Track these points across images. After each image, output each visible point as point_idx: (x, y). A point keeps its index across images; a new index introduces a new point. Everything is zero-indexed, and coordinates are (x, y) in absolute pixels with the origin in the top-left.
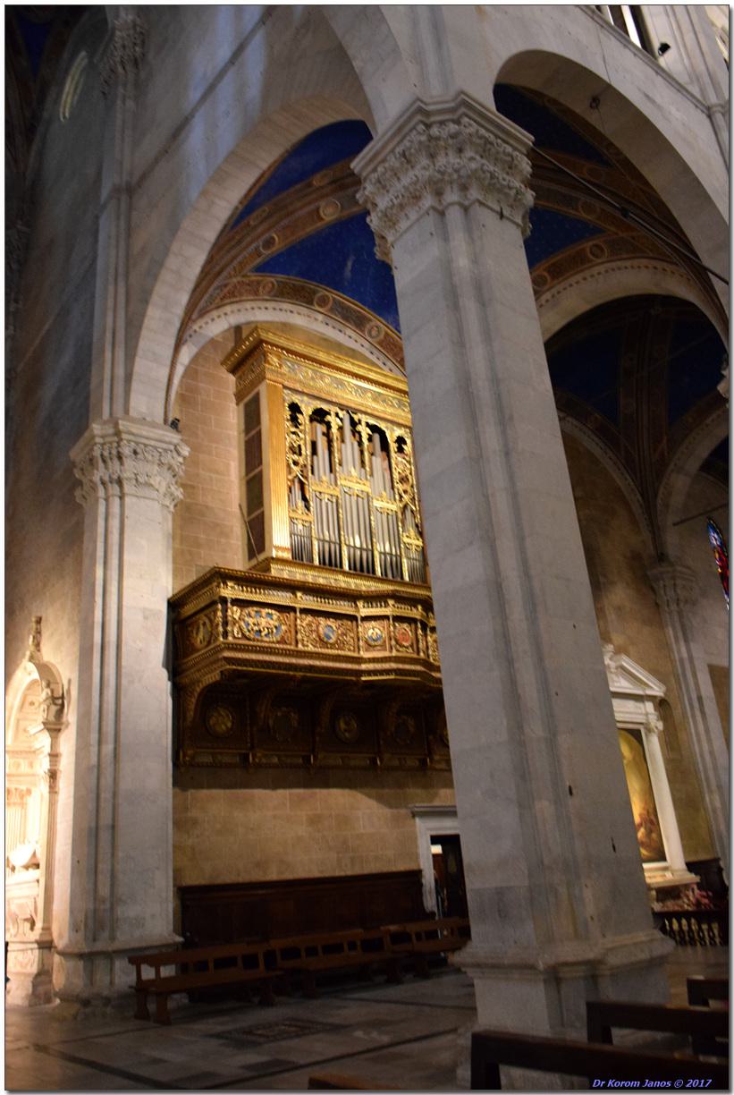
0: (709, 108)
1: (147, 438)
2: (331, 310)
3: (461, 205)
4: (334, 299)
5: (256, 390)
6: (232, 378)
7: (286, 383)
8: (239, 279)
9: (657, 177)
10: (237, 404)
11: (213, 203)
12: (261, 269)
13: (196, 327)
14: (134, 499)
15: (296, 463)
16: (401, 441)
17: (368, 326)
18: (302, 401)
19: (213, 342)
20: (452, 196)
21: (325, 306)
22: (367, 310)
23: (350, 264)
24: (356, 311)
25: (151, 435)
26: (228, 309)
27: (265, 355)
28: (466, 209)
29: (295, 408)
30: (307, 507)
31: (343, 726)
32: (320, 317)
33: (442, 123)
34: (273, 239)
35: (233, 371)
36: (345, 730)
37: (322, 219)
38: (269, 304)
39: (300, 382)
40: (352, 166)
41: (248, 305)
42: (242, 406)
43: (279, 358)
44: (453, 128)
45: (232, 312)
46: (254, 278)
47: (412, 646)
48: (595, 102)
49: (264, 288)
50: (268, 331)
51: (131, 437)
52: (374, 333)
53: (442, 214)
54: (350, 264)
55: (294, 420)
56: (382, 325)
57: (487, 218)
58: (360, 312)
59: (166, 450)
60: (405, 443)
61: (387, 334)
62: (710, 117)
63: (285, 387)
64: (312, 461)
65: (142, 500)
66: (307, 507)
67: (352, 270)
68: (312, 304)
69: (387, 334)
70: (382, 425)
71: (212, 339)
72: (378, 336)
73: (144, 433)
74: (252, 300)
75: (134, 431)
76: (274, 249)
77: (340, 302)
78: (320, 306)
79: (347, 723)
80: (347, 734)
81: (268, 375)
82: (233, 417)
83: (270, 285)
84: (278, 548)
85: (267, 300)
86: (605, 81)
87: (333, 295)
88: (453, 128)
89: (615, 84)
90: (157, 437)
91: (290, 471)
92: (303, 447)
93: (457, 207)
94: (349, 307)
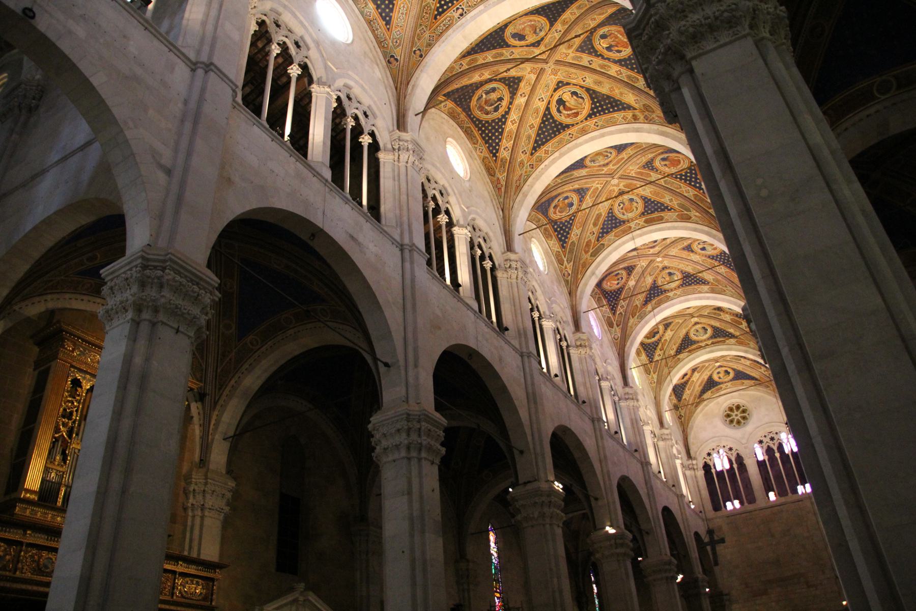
0: (402, 245)
3: (150, 321)
5: (48, 365)
6: (36, 349)
7: (74, 364)
9: (352, 287)
10: (34, 370)
13: (16, 308)
15: (64, 425)
18: (84, 378)
19: (28, 320)
20: (146, 315)
26: (49, 297)
27: (63, 340)
28: (153, 324)
29: (76, 383)
30: (64, 460)
33: (155, 267)
35: (38, 344)
38: (85, 298)
39: (86, 363)
40: (101, 272)
41: (67, 296)
42: (36, 372)
43: (75, 344)
44: (159, 273)
45: (52, 299)
48: (313, 235)
50: (69, 325)
53: (138, 324)
55: (73, 394)
57: (166, 333)
62: (402, 250)
63: (72, 366)
64: (79, 425)
66: (64, 460)
71: (29, 318)
74: (72, 293)
81: (61, 355)
82: (28, 380)
84: (28, 491)
85: (84, 294)
86: (319, 227)
88: (159, 273)
89: (326, 229)
91: (57, 430)
92: (75, 413)
93: (147, 323)
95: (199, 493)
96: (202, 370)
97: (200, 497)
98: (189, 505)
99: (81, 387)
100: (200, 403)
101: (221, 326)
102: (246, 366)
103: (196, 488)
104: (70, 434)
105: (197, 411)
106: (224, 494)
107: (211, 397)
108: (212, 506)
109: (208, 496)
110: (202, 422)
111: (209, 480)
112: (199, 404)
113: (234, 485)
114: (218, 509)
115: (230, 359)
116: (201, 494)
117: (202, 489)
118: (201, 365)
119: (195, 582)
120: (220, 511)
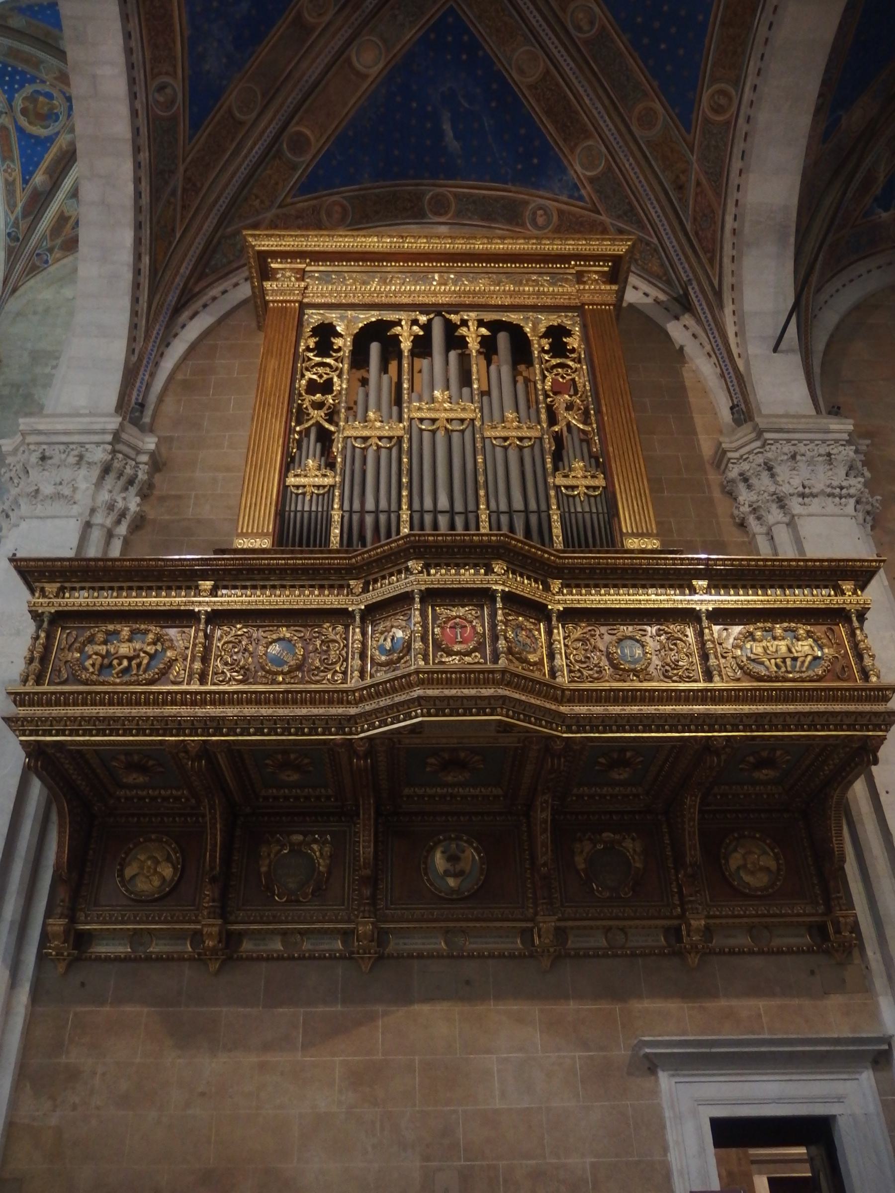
1: (66, 433)
2: (459, 214)
4: (455, 195)
8: (274, 211)
11: (94, 76)
12: (308, 186)
14: (35, 523)
16: (557, 334)
17: (528, 213)
21: (446, 213)
22: (513, 188)
23: (447, 127)
24: (497, 199)
25: (71, 427)
29: (325, 332)
31: (439, 861)
32: (443, 229)
34: (299, 134)
36: (447, 873)
37: (364, 77)
46: (303, 203)
47: (479, 648)
49: (329, 215)
51: (42, 438)
52: (540, 221)
54: (447, 127)
56: (548, 203)
58: (503, 198)
59: (98, 444)
60: (569, 334)
61: (561, 212)
65: (49, 521)
67: (457, 137)
68: (424, 216)
69: (561, 212)
70: (514, 317)
72: (549, 222)
73: (59, 427)
75: (41, 427)
76: (313, 150)
77: (464, 194)
78: (441, 215)
79: (452, 858)
80: (452, 882)
83: (337, 208)
87: (452, 189)
90: (80, 427)
94: (484, 197)
95: (758, 475)
96: (656, 250)
97: (764, 482)
98: (746, 509)
99: (339, 335)
100: (687, 316)
101: (634, 129)
102: (737, 165)
103: (745, 466)
104: (331, 417)
105: (688, 334)
106: (829, 455)
107: (700, 284)
108: (804, 487)
109: (783, 471)
110: (708, 348)
111: (767, 435)
112: (687, 319)
113: (851, 427)
114: (829, 490)
115: (698, 184)
116: (765, 474)
117: (761, 461)
118: (648, 244)
119: (778, 631)
120: (837, 494)
